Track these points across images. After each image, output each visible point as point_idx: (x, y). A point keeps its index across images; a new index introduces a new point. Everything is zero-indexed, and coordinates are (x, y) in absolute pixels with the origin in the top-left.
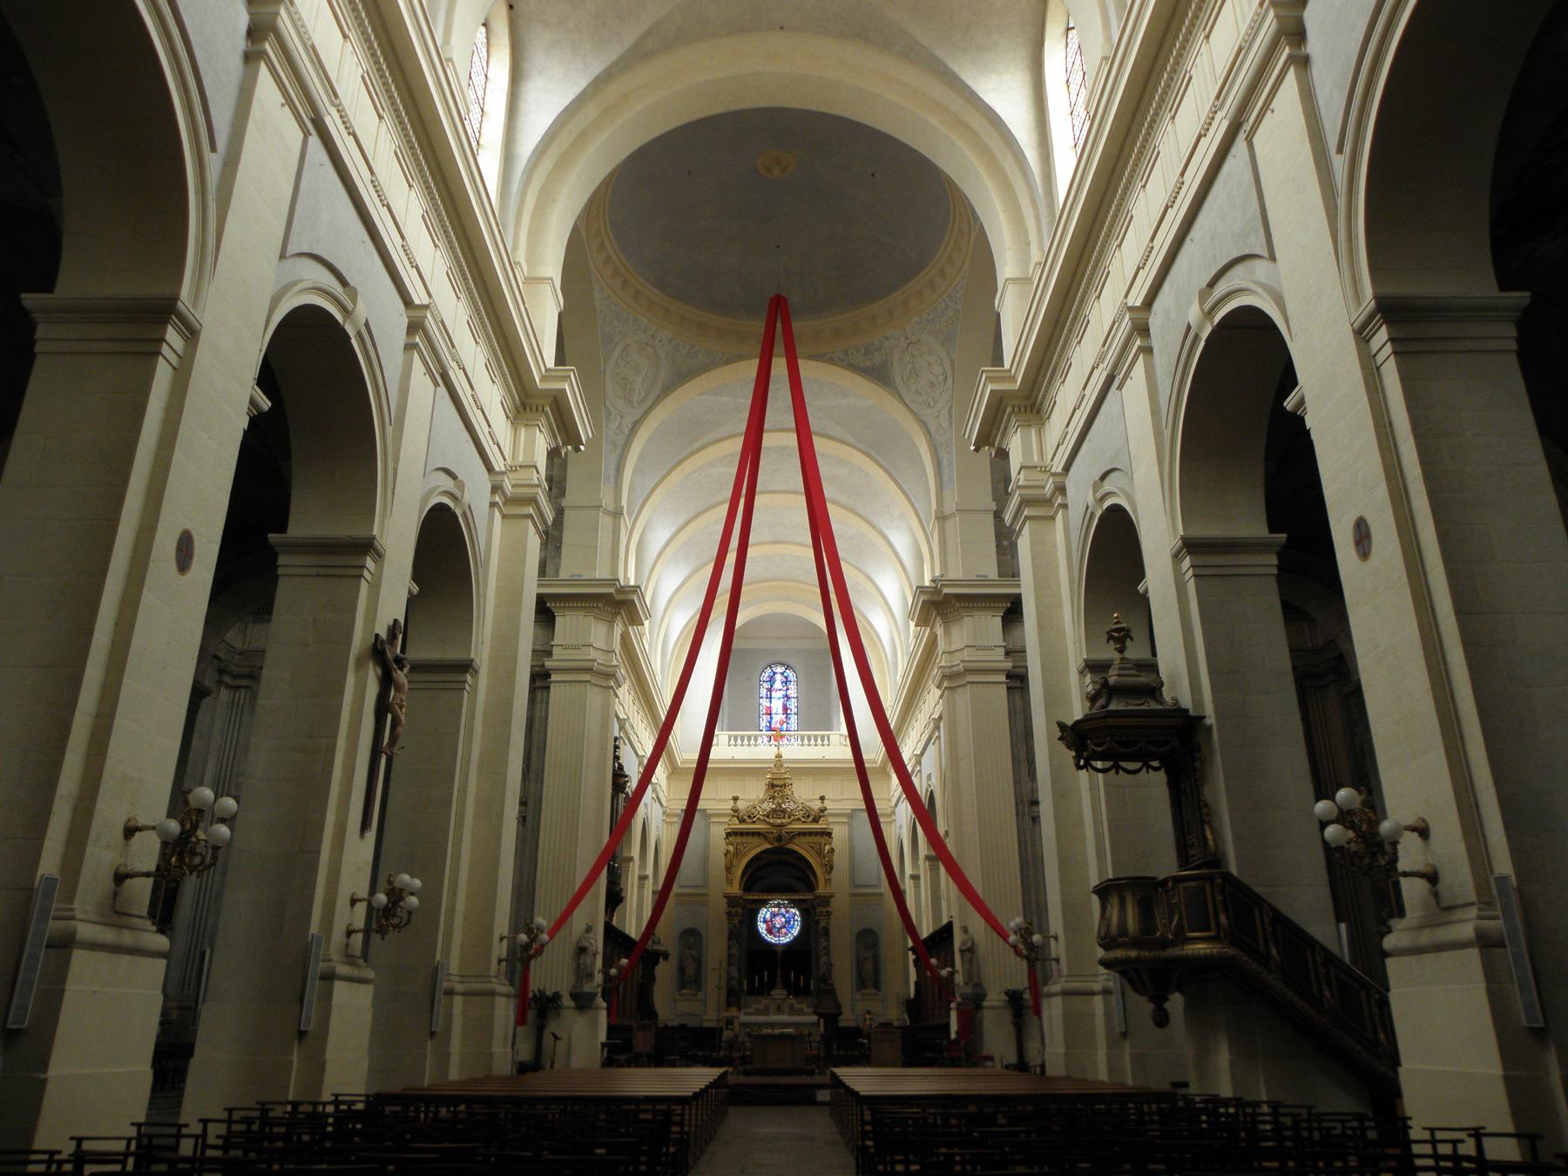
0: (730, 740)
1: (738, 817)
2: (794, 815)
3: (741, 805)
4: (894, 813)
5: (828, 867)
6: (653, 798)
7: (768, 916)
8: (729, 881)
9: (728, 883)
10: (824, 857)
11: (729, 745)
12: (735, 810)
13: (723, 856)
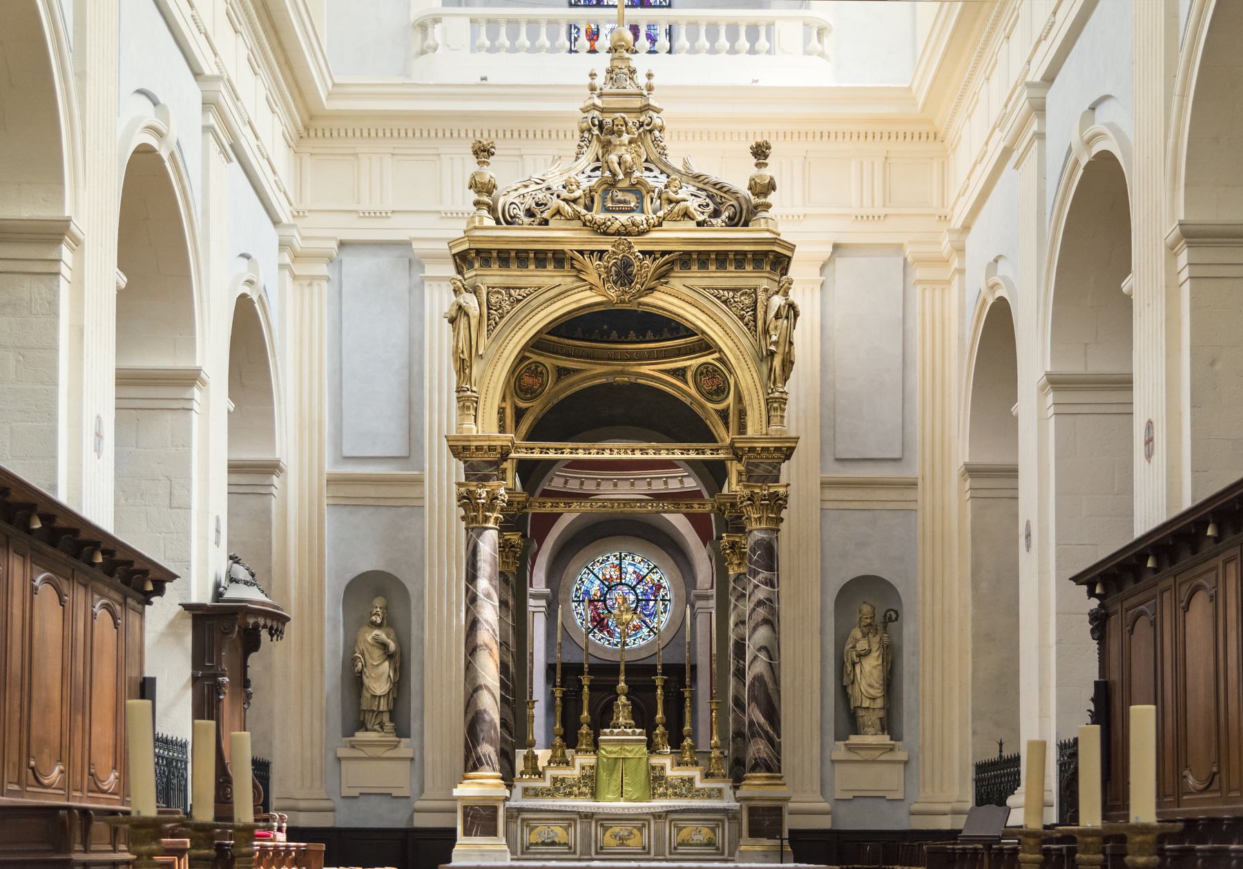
0: (474, 36)
1: (492, 210)
2: (670, 201)
3: (492, 171)
4: (960, 250)
5: (777, 362)
6: (207, 129)
7: (595, 589)
8: (467, 402)
9: (463, 408)
10: (766, 332)
11: (476, 48)
12: (483, 188)
13: (447, 326)
